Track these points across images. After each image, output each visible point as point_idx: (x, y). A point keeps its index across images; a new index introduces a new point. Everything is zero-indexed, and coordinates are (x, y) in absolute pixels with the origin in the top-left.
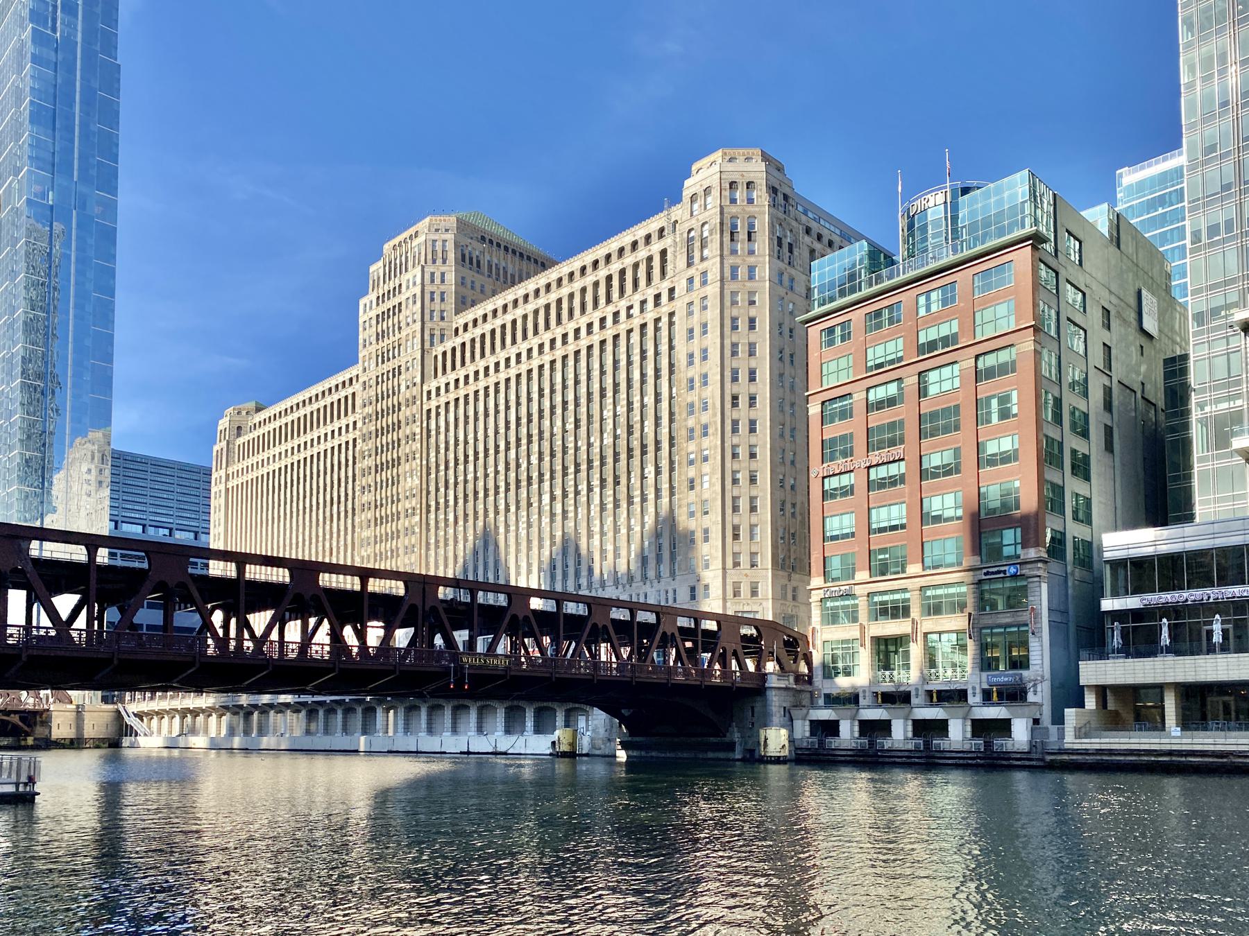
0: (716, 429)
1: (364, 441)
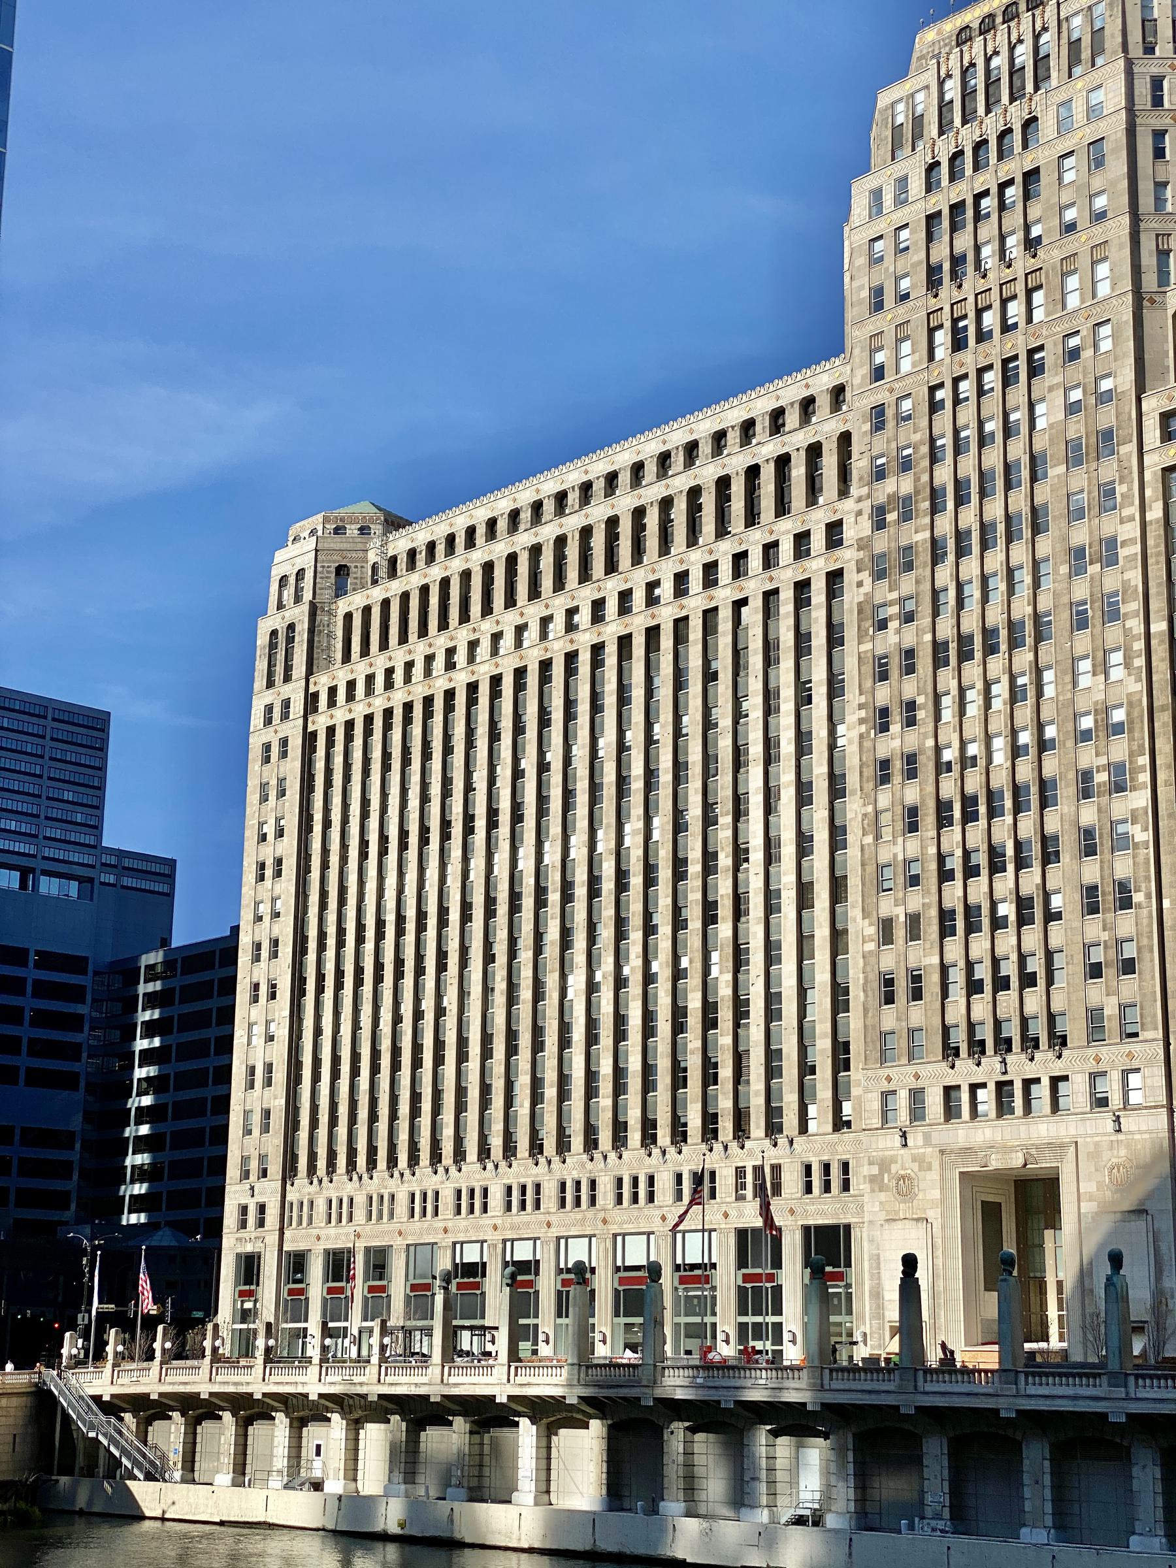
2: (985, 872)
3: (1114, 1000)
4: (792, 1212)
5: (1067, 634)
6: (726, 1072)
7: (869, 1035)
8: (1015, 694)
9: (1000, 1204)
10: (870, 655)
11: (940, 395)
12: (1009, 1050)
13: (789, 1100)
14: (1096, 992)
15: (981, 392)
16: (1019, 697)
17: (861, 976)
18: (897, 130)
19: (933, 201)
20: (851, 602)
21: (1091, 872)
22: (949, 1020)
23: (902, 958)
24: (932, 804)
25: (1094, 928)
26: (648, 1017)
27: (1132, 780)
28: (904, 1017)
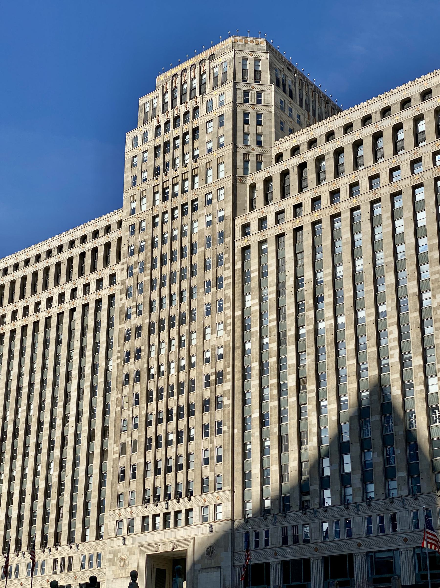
1: (129, 295)
2: (164, 421)
3: (213, 474)
4: (76, 578)
5: (202, 317)
6: (52, 516)
7: (113, 495)
8: (181, 344)
9: (165, 570)
10: (123, 329)
11: (157, 220)
12: (170, 498)
13: (78, 527)
15: (173, 218)
16: (182, 345)
17: (112, 469)
18: (146, 114)
19: (157, 141)
20: (118, 307)
21: (207, 418)
22: (147, 487)
23: (129, 460)
24: (145, 392)
25: (207, 443)
26: (22, 493)
28: (128, 487)
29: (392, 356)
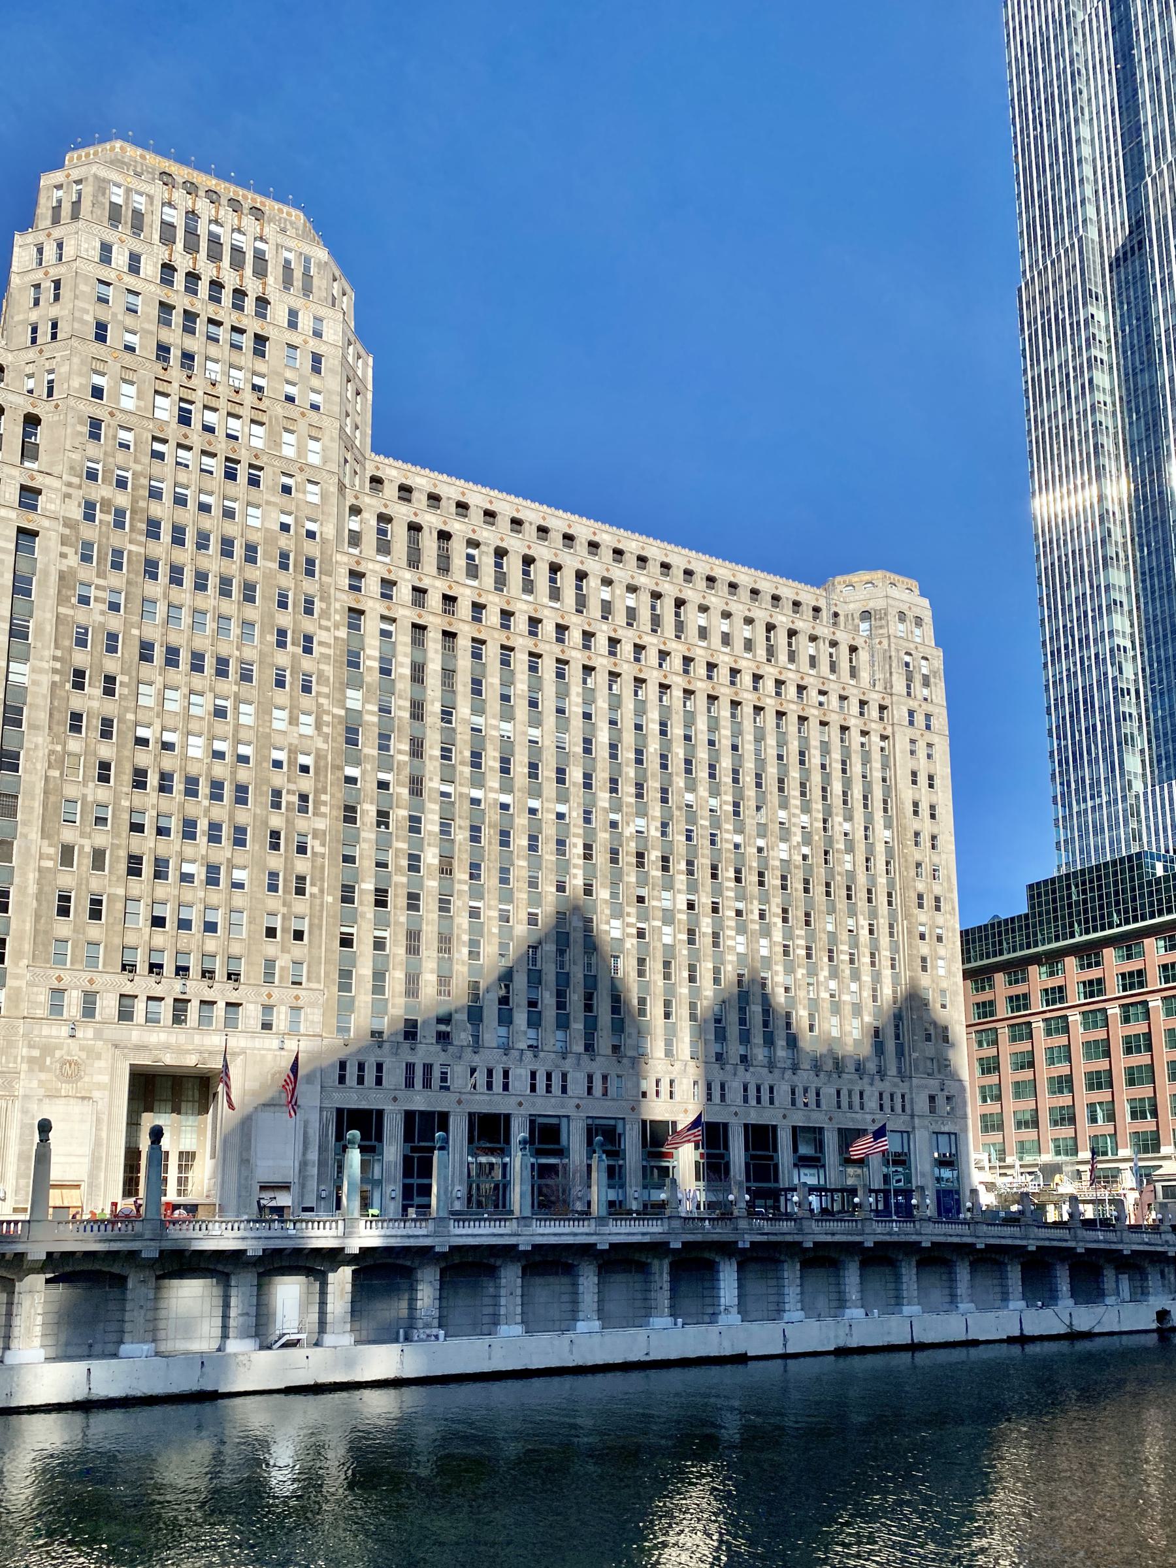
0: (953, 909)
14: (271, 948)
25: (273, 902)
27: (315, 808)
29: (575, 876)
